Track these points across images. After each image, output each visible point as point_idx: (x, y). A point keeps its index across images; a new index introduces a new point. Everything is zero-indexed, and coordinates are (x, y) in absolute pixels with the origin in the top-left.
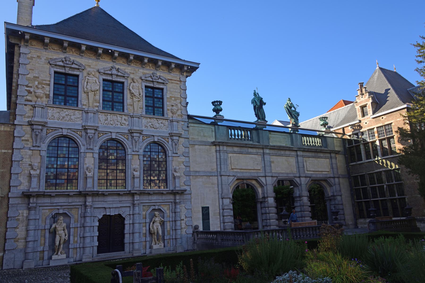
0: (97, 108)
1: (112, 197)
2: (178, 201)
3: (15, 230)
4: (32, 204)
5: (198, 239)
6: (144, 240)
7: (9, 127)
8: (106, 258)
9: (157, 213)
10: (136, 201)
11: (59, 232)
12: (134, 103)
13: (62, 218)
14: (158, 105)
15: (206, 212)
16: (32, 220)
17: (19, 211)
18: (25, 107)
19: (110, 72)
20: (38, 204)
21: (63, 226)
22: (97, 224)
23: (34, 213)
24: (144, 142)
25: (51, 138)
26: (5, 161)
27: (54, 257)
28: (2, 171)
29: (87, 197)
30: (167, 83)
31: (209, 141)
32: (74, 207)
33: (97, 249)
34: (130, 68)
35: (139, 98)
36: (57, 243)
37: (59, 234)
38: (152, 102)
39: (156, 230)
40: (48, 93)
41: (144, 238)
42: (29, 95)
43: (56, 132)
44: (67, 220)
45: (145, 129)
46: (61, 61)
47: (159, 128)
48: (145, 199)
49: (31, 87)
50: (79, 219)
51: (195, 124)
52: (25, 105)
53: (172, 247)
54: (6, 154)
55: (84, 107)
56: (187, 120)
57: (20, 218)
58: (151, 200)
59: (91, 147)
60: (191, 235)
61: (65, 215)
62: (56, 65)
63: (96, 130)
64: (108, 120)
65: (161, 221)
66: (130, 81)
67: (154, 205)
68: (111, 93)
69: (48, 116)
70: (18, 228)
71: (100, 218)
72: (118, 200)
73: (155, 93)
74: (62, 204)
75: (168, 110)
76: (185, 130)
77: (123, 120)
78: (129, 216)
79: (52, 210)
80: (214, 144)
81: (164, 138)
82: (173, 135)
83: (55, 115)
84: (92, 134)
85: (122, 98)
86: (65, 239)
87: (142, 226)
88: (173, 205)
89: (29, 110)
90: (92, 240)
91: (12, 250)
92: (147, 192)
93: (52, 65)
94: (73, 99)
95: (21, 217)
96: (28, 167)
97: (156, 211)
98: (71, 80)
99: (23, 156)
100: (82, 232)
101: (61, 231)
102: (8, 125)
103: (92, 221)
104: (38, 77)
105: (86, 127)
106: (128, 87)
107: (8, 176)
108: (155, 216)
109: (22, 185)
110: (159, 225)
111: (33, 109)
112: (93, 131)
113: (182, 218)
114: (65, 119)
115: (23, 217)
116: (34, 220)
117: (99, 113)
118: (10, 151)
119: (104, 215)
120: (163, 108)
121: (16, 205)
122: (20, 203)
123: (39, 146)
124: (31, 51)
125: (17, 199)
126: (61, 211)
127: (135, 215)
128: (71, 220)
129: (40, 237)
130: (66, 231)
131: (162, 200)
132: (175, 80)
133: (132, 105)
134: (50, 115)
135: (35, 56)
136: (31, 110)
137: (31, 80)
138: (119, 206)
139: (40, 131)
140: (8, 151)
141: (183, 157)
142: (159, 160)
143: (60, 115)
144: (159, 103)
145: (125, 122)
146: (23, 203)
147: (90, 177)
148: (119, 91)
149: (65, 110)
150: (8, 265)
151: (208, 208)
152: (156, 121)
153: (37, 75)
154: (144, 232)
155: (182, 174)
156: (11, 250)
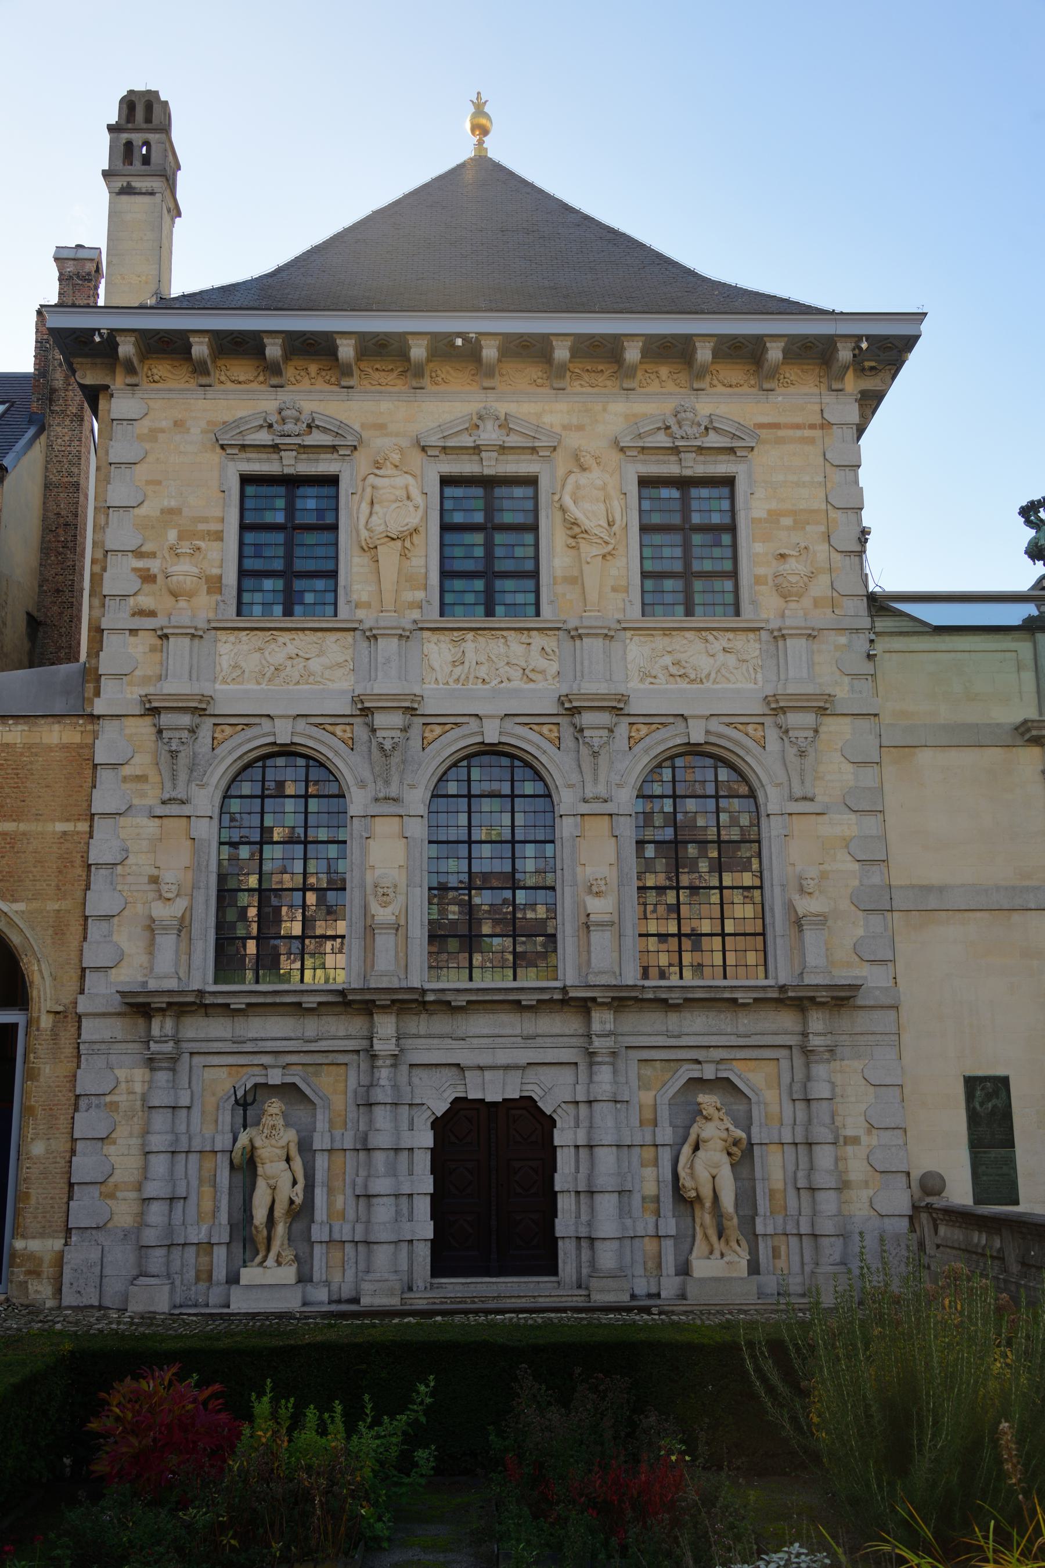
0: (416, 615)
1: (491, 1016)
2: (817, 1043)
3: (102, 1148)
4: (156, 1045)
5: (938, 1246)
6: (651, 1231)
7: (79, 728)
8: (465, 1302)
9: (708, 1100)
10: (598, 1036)
11: (267, 1166)
12: (585, 567)
13: (274, 1107)
14: (708, 566)
15: (990, 1105)
16: (161, 1110)
17: (116, 1071)
18: (132, 639)
19: (467, 441)
20: (184, 1045)
21: (283, 1142)
22: (427, 1139)
23: (168, 1081)
24: (637, 749)
25: (229, 760)
26: (65, 867)
27: (249, 1275)
28: (56, 907)
29: (376, 1018)
30: (752, 448)
31: (1002, 720)
32: (331, 1057)
33: (428, 1252)
34: (562, 406)
36: (260, 1215)
37: (267, 1178)
38: (678, 552)
39: (710, 1186)
40: (216, 571)
41: (651, 1220)
42: (147, 588)
43: (250, 732)
44: (300, 1113)
45: (642, 686)
46: (261, 426)
47: (713, 675)
48: (648, 1029)
49: (153, 555)
50: (350, 1116)
51: (915, 639)
52: (130, 635)
53: (799, 1279)
54: (69, 838)
55: (361, 614)
56: (866, 622)
57: (120, 1098)
58: (679, 1036)
59: (393, 791)
60: (905, 1223)
61: (290, 1091)
62: (243, 447)
63: (411, 711)
64: (467, 664)
65: (730, 1140)
67: (698, 1062)
68: (478, 538)
69: (218, 668)
70: (115, 1143)
71: (439, 1114)
72: (518, 1032)
73: (695, 505)
74: (278, 1043)
75: (759, 580)
76: (855, 676)
77: (532, 653)
78: (571, 1109)
79: (240, 1069)
80: (1027, 736)
81: (740, 726)
82: (782, 704)
83: (243, 664)
84: (393, 734)
85: (530, 552)
86: (292, 1202)
87: (635, 1160)
88: (798, 1061)
89: (144, 653)
90: (405, 1211)
91: (94, 1232)
92: (651, 996)
93: (229, 451)
94: (320, 584)
95: (124, 1098)
96: (147, 887)
97: (711, 1092)
98: (309, 501)
99: (128, 843)
100: (363, 1173)
101: (273, 1164)
102: (74, 720)
103: (405, 1126)
105: (367, 705)
106: (556, 498)
107: (76, 928)
108: (697, 1113)
109: (124, 963)
110: (725, 1159)
111: (159, 647)
112: (397, 719)
113: (849, 1132)
114: (283, 674)
115: (131, 1097)
116: (165, 1110)
117: (426, 634)
118: (83, 827)
119: (457, 1099)
120: (734, 575)
121: (103, 1046)
122: (119, 1038)
123: (184, 798)
124: (151, 403)
125: (109, 1021)
126: (275, 1077)
127: (596, 1106)
128: (314, 1116)
129: (194, 1183)
130: (298, 1164)
131: (739, 1036)
132: (798, 427)
133: (575, 580)
134: (225, 665)
135: (164, 424)
136: (153, 649)
137: (153, 527)
138: (523, 1061)
139: (185, 734)
140: (75, 826)
141: (845, 816)
142: (719, 834)
143: (264, 662)
144: (717, 552)
145: (542, 663)
146: (129, 1037)
147: (386, 926)
148: (519, 519)
149: (285, 637)
150: (79, 1292)
151: (1005, 1081)
152: (700, 645)
153: (173, 504)
154: (650, 1189)
156: (89, 1231)
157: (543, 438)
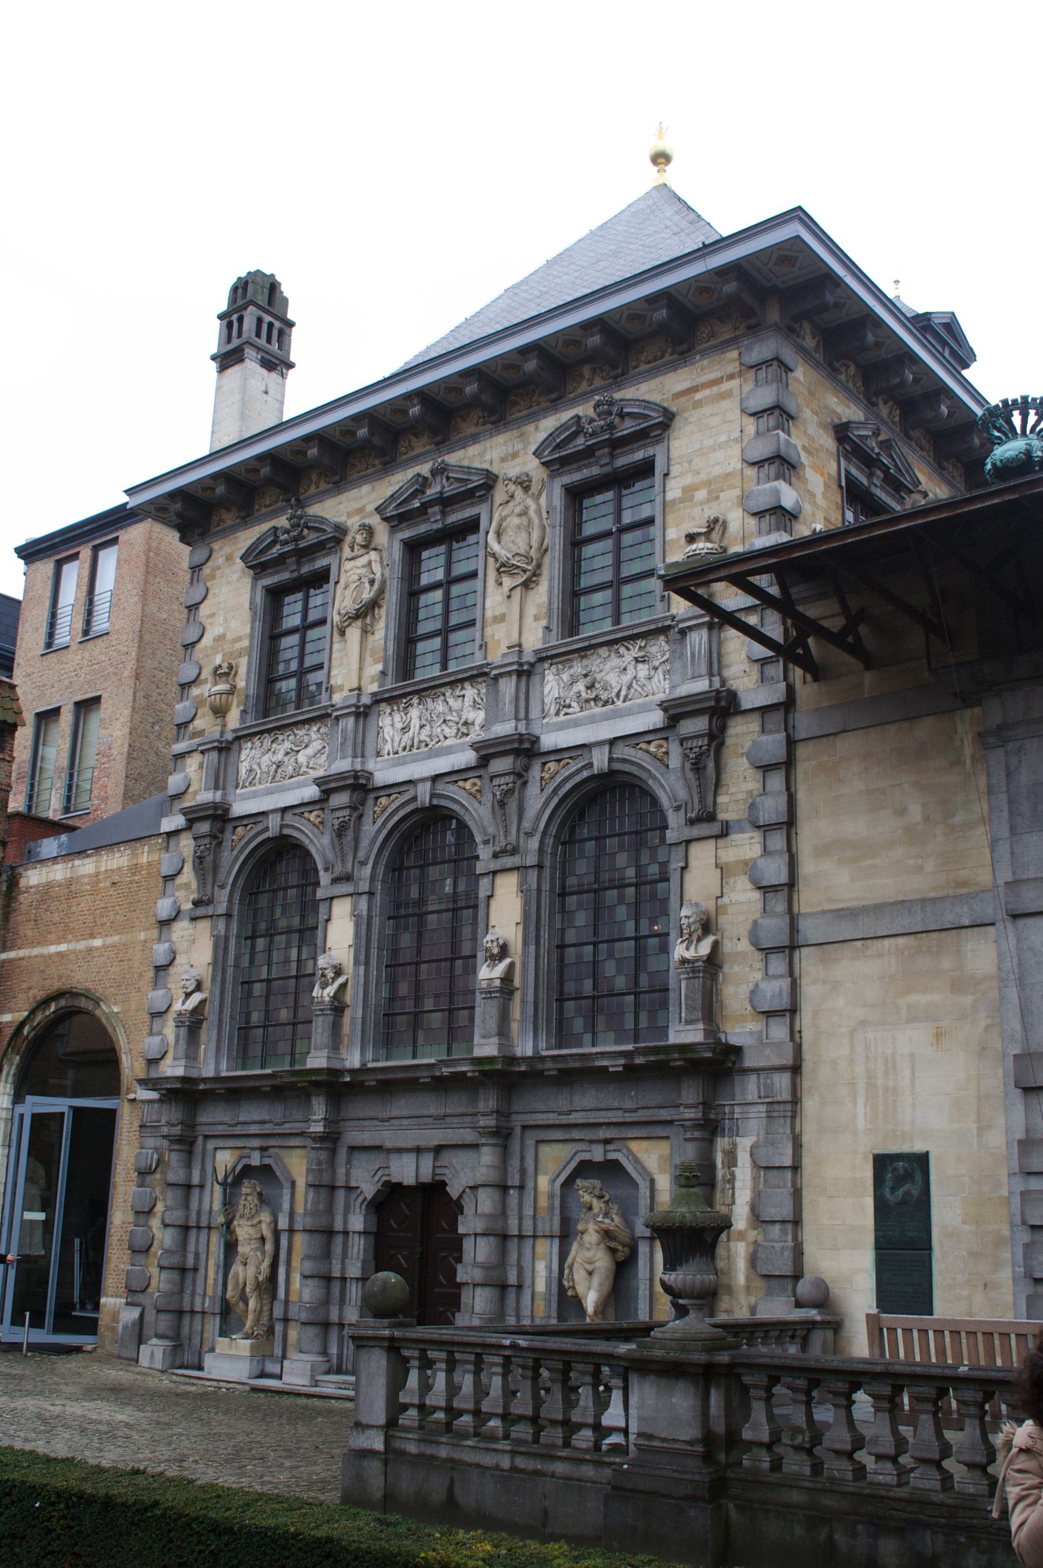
15: (900, 1192)
22: (357, 1222)
34: (501, 439)
49: (206, 681)
58: (569, 1113)
61: (265, 1172)
66: (499, 494)
104: (221, 638)
141: (748, 835)
151: (922, 1161)
155: (744, 945)
157: (475, 478)
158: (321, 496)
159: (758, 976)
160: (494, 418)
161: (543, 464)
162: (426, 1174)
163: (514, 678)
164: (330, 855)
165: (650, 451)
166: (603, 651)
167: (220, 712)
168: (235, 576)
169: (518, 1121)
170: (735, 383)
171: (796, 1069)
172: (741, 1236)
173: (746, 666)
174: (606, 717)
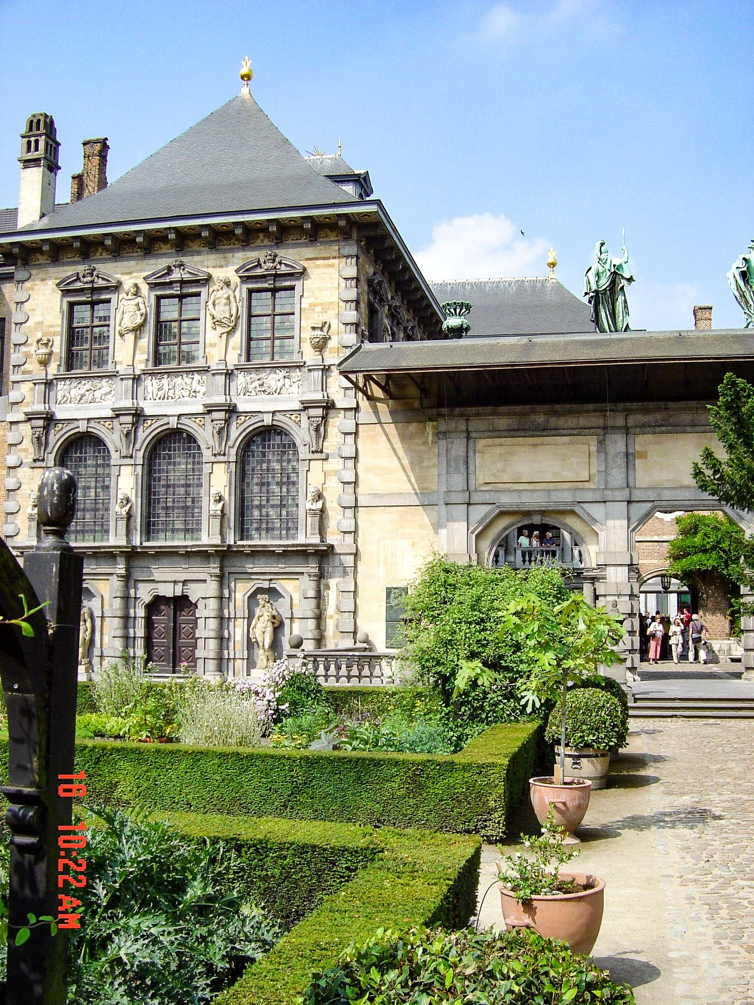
35: (229, 326)
49: (31, 345)
104: (42, 323)
153: (40, 320)
155: (335, 504)
157: (201, 275)
158: (104, 261)
159: (341, 517)
160: (210, 247)
161: (240, 277)
162: (179, 593)
163: (224, 376)
164: (119, 445)
165: (293, 283)
166: (268, 371)
167: (45, 363)
168: (48, 292)
169: (227, 570)
170: (336, 261)
171: (356, 555)
172: (331, 617)
173: (338, 389)
174: (270, 401)
